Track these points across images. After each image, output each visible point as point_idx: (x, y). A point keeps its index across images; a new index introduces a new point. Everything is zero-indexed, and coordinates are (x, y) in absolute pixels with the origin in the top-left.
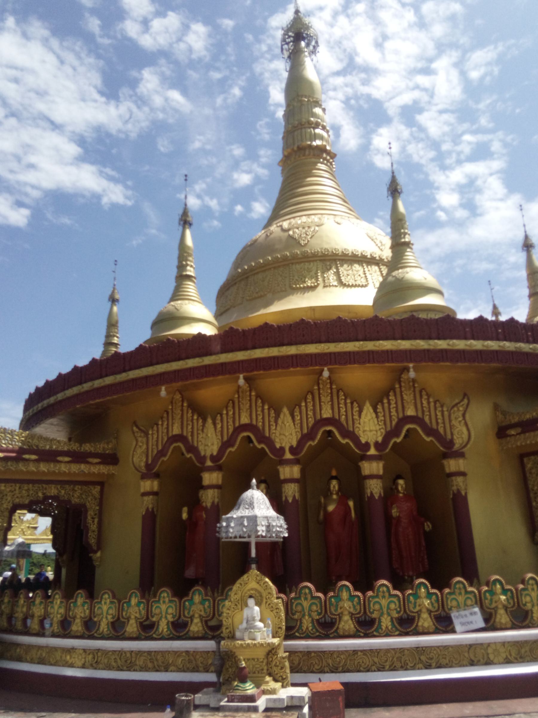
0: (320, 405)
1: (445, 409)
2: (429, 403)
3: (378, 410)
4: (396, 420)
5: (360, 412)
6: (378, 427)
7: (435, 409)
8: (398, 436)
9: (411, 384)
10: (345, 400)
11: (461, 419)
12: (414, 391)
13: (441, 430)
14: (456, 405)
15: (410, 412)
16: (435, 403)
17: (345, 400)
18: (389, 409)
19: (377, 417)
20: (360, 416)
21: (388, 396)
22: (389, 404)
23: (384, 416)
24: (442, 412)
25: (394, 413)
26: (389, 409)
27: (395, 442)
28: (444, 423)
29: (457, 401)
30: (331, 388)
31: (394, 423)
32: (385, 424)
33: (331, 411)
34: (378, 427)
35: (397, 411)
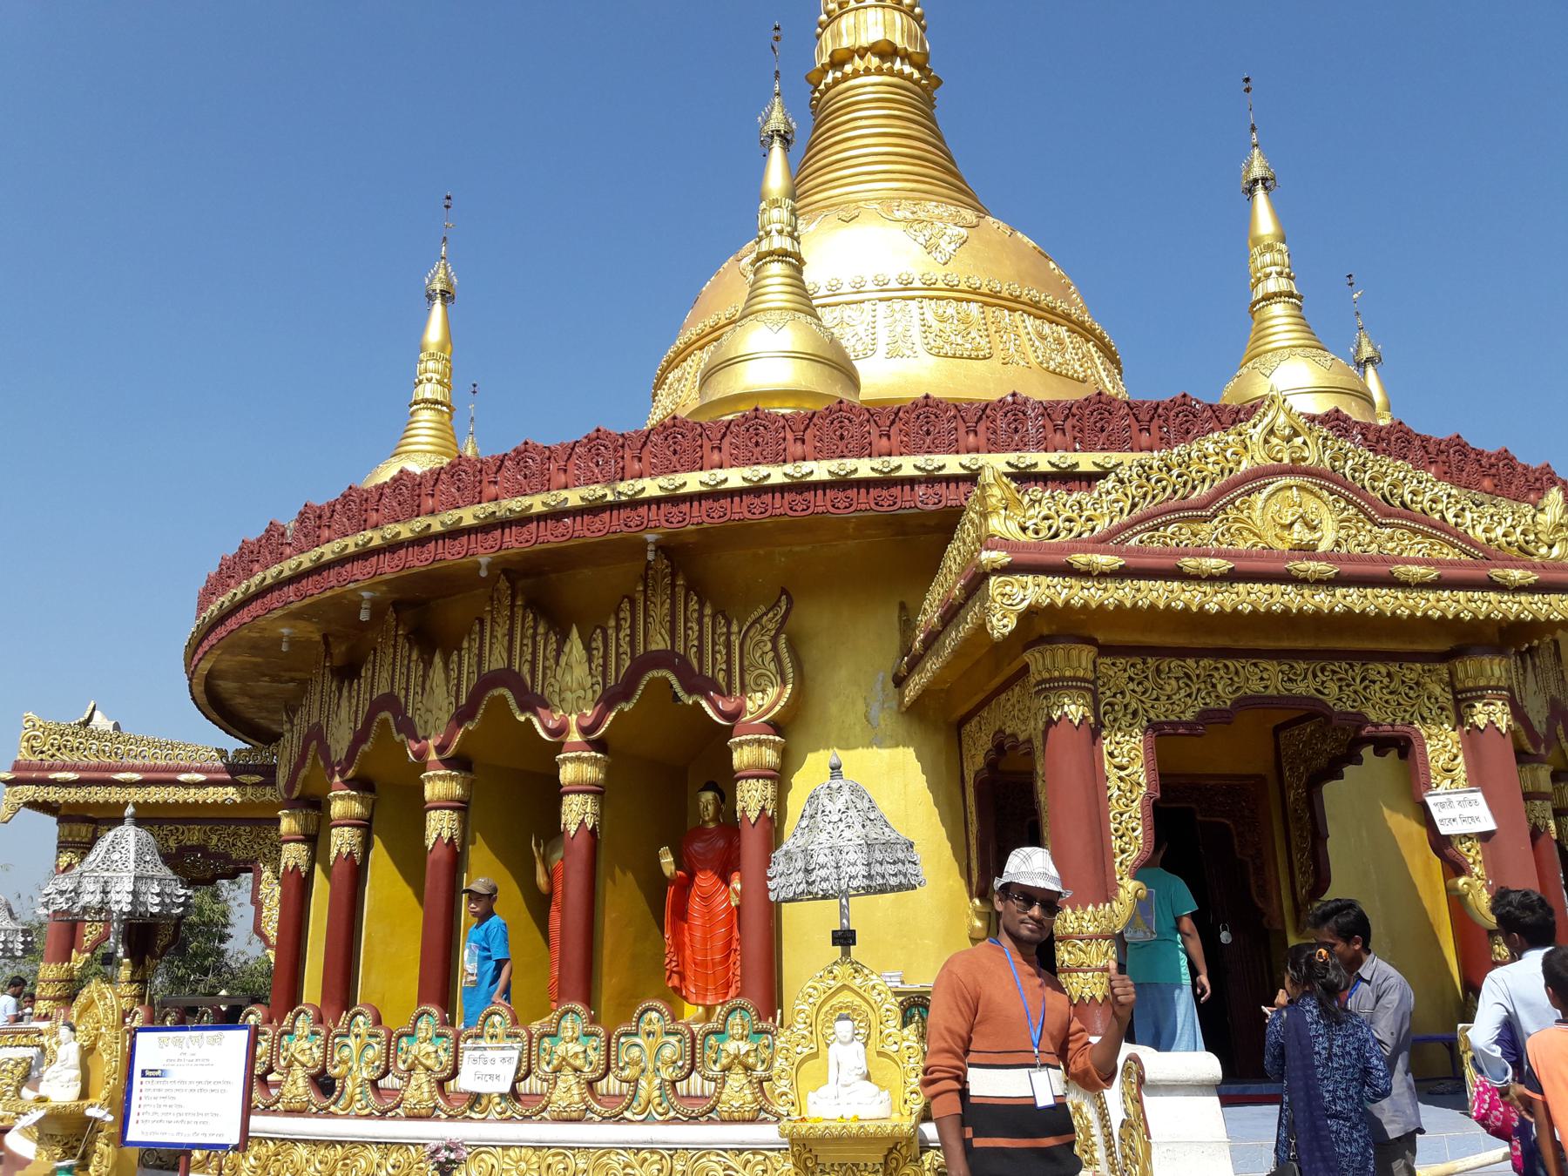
0: (491, 644)
1: (735, 628)
2: (700, 622)
3: (594, 645)
4: (628, 663)
5: (559, 651)
6: (589, 681)
7: (714, 633)
8: (627, 699)
9: (667, 580)
10: (535, 628)
11: (769, 645)
12: (673, 597)
13: (721, 676)
14: (761, 617)
15: (659, 643)
16: (714, 617)
17: (535, 628)
18: (618, 639)
19: (590, 660)
20: (557, 663)
21: (618, 610)
22: (618, 628)
23: (605, 657)
24: (729, 634)
25: (625, 647)
26: (618, 639)
27: (621, 712)
28: (729, 662)
29: (763, 609)
30: (512, 606)
31: (623, 671)
32: (605, 675)
33: (505, 656)
34: (589, 681)
35: (632, 644)
